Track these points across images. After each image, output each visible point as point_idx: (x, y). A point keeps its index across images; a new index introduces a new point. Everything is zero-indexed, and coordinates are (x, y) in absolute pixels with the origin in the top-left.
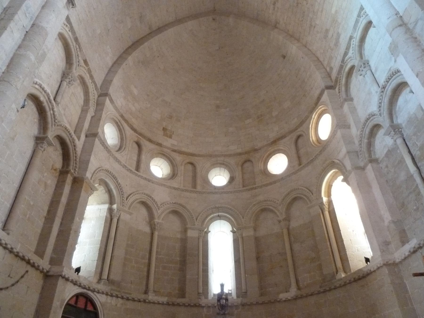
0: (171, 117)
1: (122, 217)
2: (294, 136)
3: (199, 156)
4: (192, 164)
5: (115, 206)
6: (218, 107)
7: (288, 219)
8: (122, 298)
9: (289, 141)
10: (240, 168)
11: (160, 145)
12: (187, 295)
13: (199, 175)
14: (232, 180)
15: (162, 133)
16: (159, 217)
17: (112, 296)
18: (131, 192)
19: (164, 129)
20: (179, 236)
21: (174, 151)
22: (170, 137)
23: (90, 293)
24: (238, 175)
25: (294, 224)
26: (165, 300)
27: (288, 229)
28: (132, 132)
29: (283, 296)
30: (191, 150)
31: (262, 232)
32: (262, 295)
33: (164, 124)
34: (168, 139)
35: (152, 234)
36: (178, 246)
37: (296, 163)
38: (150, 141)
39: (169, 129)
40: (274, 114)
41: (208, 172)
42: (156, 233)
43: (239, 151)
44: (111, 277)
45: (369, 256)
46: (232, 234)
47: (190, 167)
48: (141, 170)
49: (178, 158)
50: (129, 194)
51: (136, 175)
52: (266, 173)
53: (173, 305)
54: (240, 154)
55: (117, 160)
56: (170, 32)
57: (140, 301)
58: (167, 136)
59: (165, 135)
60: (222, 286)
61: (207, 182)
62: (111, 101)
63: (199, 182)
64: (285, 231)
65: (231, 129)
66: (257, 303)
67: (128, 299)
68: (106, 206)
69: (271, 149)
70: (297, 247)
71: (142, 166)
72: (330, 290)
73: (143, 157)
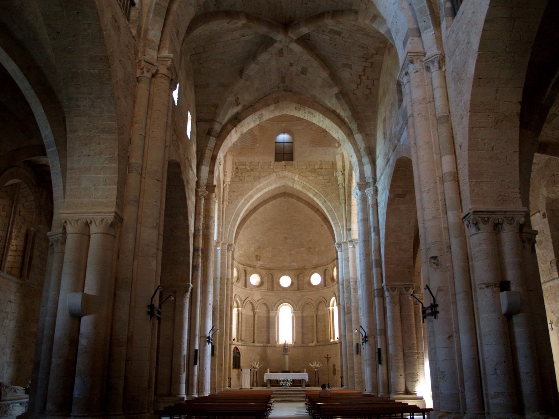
0: (259, 248)
1: (243, 313)
2: (324, 268)
3: (275, 269)
4: (271, 274)
5: (240, 309)
6: (286, 238)
7: (317, 309)
8: (246, 346)
9: (322, 269)
10: (296, 278)
11: (254, 267)
12: (271, 342)
13: (275, 282)
14: (292, 284)
15: (255, 259)
16: (257, 308)
17: (243, 345)
18: (245, 299)
19: (256, 256)
20: (266, 315)
21: (262, 269)
22: (260, 260)
23: (237, 346)
24: (296, 282)
25: (319, 313)
26: (262, 345)
27: (317, 315)
28: (242, 266)
29: (311, 344)
30: (271, 265)
31: (305, 314)
32: (303, 343)
33: (256, 253)
34: (259, 262)
35: (254, 316)
36: (265, 320)
37: (323, 284)
38: (250, 267)
39: (259, 255)
40: (317, 250)
41: (279, 278)
42: (256, 316)
43: (297, 267)
44: (242, 339)
45: (338, 337)
46: (291, 313)
47: (270, 276)
48: (248, 286)
49: (264, 272)
50: (244, 300)
51: (246, 289)
52: (309, 283)
53: (265, 346)
54: (297, 269)
55: (239, 287)
56: (261, 210)
57: (252, 346)
58: (258, 260)
59: (257, 260)
60: (286, 341)
61: (279, 284)
62: (235, 260)
63: (275, 286)
64: (315, 317)
65: (293, 252)
66: (300, 346)
67: (248, 346)
68: (237, 309)
69: (313, 271)
70: (319, 324)
71: (248, 283)
72: (327, 345)
73: (248, 278)
